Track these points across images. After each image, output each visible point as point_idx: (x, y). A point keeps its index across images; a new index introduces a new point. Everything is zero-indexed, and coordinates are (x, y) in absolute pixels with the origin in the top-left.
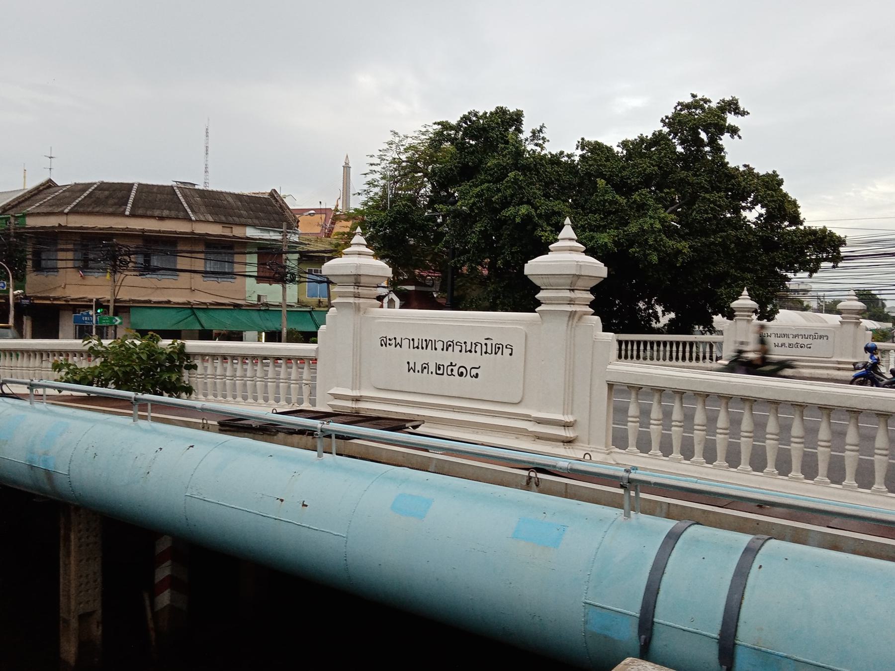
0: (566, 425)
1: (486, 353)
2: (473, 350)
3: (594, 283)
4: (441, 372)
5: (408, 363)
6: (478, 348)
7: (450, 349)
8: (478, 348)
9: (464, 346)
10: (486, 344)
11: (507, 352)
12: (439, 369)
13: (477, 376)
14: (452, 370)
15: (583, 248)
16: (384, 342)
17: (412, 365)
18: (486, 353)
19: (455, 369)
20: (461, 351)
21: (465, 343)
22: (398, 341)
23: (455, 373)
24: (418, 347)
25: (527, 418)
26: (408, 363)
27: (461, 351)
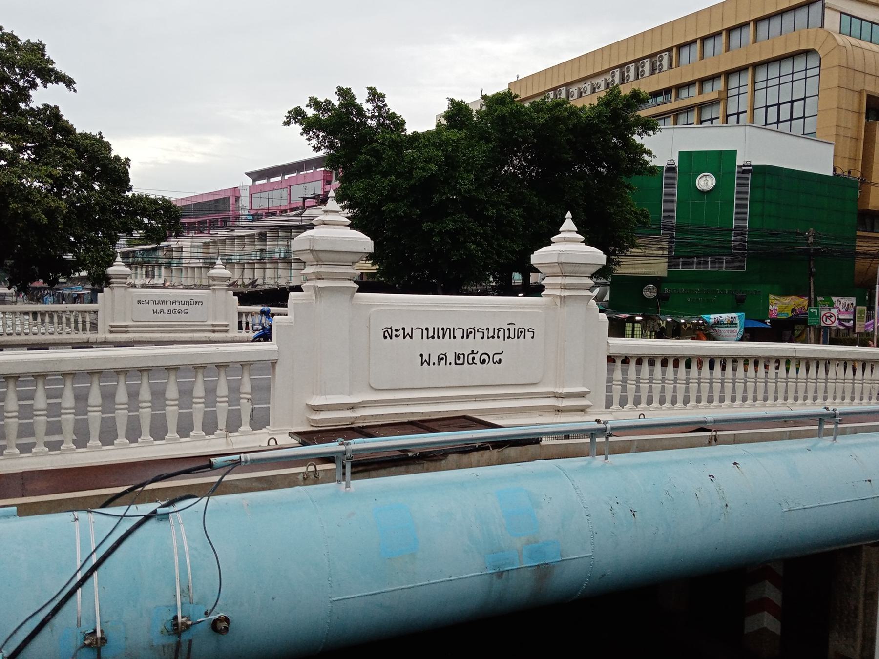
0: (582, 395)
1: (509, 337)
2: (496, 336)
3: (594, 270)
4: (461, 361)
5: (421, 355)
6: (501, 334)
7: (471, 336)
8: (501, 334)
9: (486, 332)
10: (509, 329)
11: (529, 335)
12: (459, 358)
13: (500, 361)
14: (473, 358)
15: (582, 238)
16: (388, 334)
17: (426, 357)
18: (509, 337)
19: (477, 357)
20: (483, 338)
21: (488, 329)
22: (408, 331)
23: (477, 360)
24: (433, 337)
25: (547, 395)
26: (421, 355)
27: (483, 338)
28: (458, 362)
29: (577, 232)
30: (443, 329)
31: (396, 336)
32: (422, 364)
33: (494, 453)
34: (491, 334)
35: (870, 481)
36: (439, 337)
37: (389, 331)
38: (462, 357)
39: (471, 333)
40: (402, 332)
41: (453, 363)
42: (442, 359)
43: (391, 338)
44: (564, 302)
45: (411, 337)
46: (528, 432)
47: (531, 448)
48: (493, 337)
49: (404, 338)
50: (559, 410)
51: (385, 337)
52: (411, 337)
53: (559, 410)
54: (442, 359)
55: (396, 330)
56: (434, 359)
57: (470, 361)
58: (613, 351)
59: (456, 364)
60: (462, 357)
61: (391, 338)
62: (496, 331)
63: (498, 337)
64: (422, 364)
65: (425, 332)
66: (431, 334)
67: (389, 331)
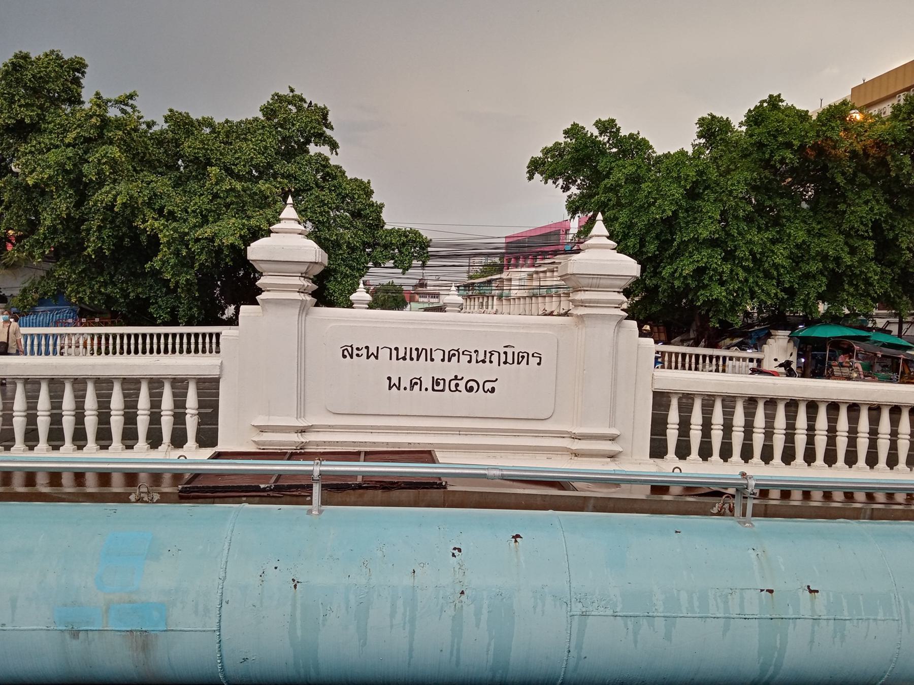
0: (613, 438)
1: (505, 363)
2: (487, 360)
4: (441, 387)
5: (389, 378)
6: (495, 358)
7: (454, 359)
8: (495, 358)
9: (474, 355)
10: (505, 353)
11: (534, 361)
12: (438, 384)
13: (493, 390)
14: (457, 385)
15: (613, 244)
16: (348, 352)
17: (395, 381)
18: (505, 363)
19: (462, 384)
20: (470, 362)
21: (476, 351)
22: (373, 350)
23: (462, 387)
24: (404, 358)
25: (561, 435)
26: (389, 378)
27: (470, 362)
28: (436, 388)
29: (608, 238)
30: (417, 349)
31: (358, 355)
32: (390, 388)
33: (412, 492)
34: (481, 357)
35: (771, 591)
36: (412, 359)
37: (350, 349)
38: (442, 382)
39: (454, 355)
40: (364, 351)
41: (430, 388)
42: (416, 383)
43: (352, 357)
44: (583, 321)
45: (377, 357)
46: (537, 476)
47: (434, 493)
48: (484, 361)
49: (368, 357)
50: (576, 454)
51: (344, 356)
52: (377, 357)
53: (576, 454)
54: (416, 383)
55: (358, 349)
56: (405, 383)
57: (453, 388)
58: (661, 386)
59: (433, 390)
60: (442, 382)
61: (352, 357)
62: (488, 355)
63: (491, 362)
64: (390, 388)
65: (394, 352)
66: (401, 355)
67: (350, 349)
